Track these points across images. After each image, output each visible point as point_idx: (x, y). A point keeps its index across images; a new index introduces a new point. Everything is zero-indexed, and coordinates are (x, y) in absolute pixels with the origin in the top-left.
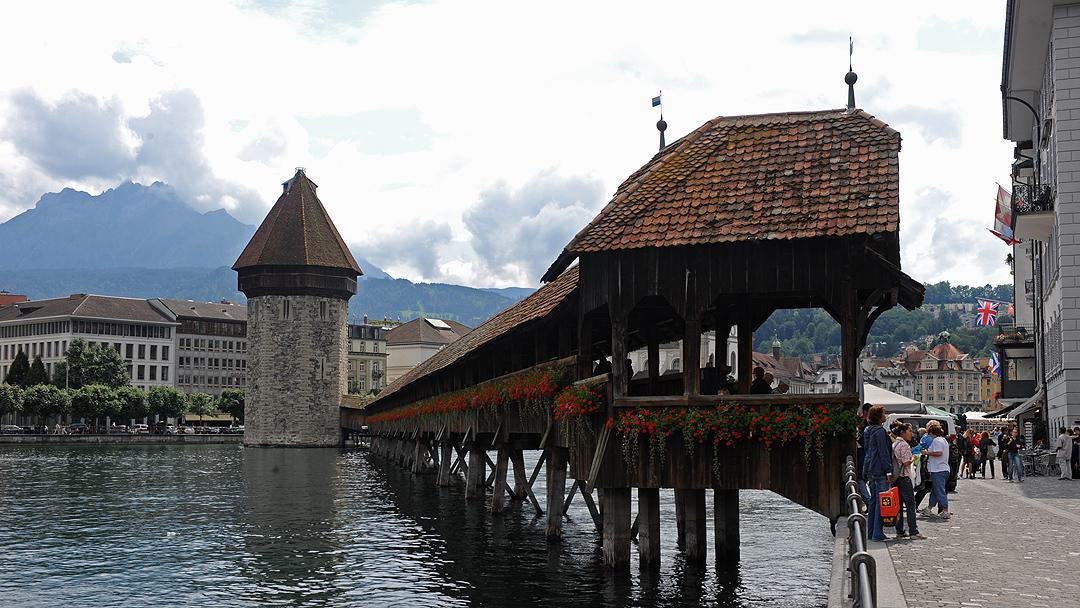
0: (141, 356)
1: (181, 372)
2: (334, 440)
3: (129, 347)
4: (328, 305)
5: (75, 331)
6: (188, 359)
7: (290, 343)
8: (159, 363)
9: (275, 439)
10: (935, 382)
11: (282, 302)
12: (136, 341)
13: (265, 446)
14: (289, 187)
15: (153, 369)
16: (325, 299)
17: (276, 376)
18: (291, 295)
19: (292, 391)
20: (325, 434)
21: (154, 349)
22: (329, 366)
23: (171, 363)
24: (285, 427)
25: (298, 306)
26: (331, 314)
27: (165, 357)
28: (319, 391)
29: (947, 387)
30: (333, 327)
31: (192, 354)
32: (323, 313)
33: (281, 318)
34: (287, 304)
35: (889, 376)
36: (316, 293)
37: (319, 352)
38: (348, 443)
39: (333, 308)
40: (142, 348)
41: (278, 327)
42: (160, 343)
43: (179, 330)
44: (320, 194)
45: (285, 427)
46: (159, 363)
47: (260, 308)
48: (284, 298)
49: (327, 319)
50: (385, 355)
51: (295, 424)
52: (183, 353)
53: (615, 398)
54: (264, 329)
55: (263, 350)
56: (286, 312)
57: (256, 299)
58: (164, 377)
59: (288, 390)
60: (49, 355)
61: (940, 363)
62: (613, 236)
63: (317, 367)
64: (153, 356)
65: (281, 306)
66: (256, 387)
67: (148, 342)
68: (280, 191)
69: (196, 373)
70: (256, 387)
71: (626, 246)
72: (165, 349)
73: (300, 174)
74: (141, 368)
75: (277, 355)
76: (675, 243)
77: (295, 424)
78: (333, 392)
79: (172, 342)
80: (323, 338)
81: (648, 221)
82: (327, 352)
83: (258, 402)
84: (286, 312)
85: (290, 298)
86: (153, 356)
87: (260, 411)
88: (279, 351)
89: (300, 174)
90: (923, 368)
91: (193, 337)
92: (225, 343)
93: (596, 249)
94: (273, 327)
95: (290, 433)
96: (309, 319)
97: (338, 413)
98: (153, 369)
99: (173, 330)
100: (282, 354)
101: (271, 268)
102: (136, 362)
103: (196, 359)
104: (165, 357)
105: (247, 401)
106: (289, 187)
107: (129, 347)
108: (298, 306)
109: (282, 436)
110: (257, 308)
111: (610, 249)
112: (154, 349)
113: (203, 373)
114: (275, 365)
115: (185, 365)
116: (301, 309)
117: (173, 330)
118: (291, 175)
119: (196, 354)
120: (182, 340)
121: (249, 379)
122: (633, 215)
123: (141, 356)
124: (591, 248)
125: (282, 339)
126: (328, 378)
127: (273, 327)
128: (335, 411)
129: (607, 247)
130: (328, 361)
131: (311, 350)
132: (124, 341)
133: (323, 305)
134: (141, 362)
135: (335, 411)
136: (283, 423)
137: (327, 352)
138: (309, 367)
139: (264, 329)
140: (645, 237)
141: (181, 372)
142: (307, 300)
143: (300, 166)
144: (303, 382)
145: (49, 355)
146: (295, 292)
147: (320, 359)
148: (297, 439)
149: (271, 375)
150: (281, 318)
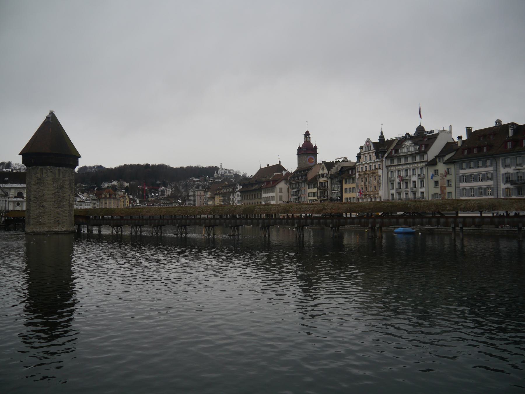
9: (55, 229)
17: (55, 201)
29: (112, 203)
33: (57, 176)
34: (59, 170)
45: (59, 224)
47: (44, 171)
51: (63, 222)
57: (40, 167)
61: (110, 195)
65: (57, 171)
66: (43, 206)
70: (43, 206)
73: (52, 113)
83: (44, 213)
85: (61, 168)
88: (56, 191)
89: (52, 113)
90: (103, 196)
100: (58, 192)
109: (57, 228)
136: (58, 222)
143: (52, 110)
146: (62, 166)
148: (64, 229)
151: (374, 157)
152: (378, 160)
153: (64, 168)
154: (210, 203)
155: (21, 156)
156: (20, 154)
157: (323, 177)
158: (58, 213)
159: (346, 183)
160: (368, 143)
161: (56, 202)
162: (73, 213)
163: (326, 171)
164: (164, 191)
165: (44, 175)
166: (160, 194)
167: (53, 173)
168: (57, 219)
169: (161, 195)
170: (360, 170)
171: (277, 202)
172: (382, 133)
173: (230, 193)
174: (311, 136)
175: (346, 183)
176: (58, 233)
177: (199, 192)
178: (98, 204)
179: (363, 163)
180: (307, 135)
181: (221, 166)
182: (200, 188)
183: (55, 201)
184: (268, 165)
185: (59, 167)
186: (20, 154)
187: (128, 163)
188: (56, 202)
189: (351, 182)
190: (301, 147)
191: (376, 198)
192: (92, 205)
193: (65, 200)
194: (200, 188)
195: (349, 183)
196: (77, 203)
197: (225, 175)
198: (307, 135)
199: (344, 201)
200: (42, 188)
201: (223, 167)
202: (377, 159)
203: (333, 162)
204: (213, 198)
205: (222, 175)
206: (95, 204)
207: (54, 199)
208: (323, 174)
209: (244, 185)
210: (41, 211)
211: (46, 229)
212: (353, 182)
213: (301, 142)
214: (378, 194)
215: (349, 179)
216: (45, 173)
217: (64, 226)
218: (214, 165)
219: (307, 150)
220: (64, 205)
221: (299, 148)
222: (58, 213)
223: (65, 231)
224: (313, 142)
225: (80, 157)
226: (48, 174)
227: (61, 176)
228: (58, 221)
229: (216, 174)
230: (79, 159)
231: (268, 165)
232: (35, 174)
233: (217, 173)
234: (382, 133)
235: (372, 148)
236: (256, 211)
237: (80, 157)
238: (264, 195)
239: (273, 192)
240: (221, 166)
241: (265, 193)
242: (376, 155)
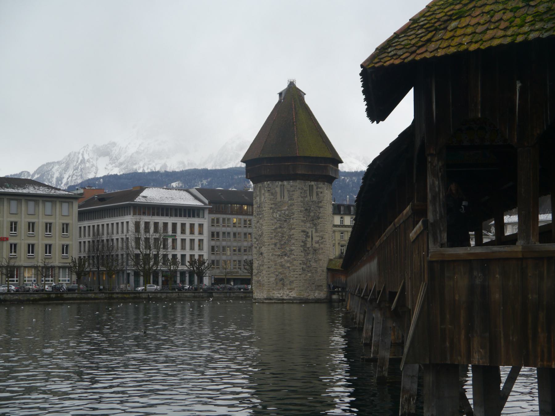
0: (183, 232)
1: (213, 243)
2: (321, 294)
3: (174, 225)
4: (315, 187)
5: (134, 214)
6: (218, 233)
7: (286, 218)
8: (196, 237)
9: (277, 294)
11: (279, 186)
12: (179, 221)
14: (283, 95)
15: (192, 241)
16: (313, 183)
17: (275, 244)
18: (286, 180)
19: (288, 257)
20: (316, 290)
21: (192, 226)
22: (317, 236)
23: (205, 236)
24: (283, 285)
25: (292, 189)
26: (317, 194)
27: (201, 233)
28: (310, 257)
30: (318, 204)
31: (221, 229)
32: (311, 194)
33: (279, 199)
36: (305, 178)
37: (308, 225)
38: (335, 297)
39: (319, 190)
40: (183, 225)
41: (276, 206)
42: (196, 221)
43: (211, 212)
44: (308, 100)
45: (283, 285)
46: (196, 237)
47: (263, 192)
48: (280, 183)
49: (315, 198)
51: (291, 282)
52: (216, 229)
53: (431, 250)
54: (266, 208)
55: (265, 223)
56: (282, 195)
57: (260, 185)
58: (201, 248)
59: (285, 255)
60: (117, 233)
62: (420, 44)
63: (307, 236)
64: (192, 232)
65: (278, 190)
67: (188, 221)
68: (276, 99)
69: (224, 243)
70: (261, 254)
71: (432, 55)
72: (201, 226)
73: (292, 85)
74: (183, 240)
75: (276, 228)
76: (496, 42)
77: (291, 282)
78: (321, 257)
79: (205, 221)
80: (312, 214)
81: (464, 21)
82: (315, 225)
84: (282, 195)
85: (285, 183)
86: (192, 232)
87: (264, 272)
89: (292, 85)
91: (221, 216)
92: (245, 221)
93: (397, 62)
94: (273, 206)
95: (288, 289)
96: (300, 199)
97: (325, 273)
98: (192, 241)
99: (206, 212)
100: (280, 227)
101: (270, 160)
102: (179, 236)
103: (224, 233)
104: (201, 233)
105: (255, 265)
106: (283, 95)
107: (174, 225)
108: (292, 189)
109: (281, 291)
110: (260, 191)
111: (413, 60)
112: (192, 226)
113: (229, 244)
114: (275, 236)
115: (215, 238)
116: (294, 191)
117: (206, 212)
118: (284, 86)
119: (224, 229)
120: (213, 220)
121: (256, 248)
122: (446, 18)
123: (183, 232)
124: (391, 62)
125: (280, 216)
126: (317, 246)
127: (273, 206)
128: (323, 271)
129: (410, 59)
130: (316, 231)
131: (303, 224)
132: (170, 220)
133: (311, 187)
134: (183, 237)
135: (323, 271)
136: (281, 282)
137: (315, 225)
138: (301, 236)
139: (266, 208)
140: (457, 40)
141: (213, 243)
142: (298, 184)
143: (292, 78)
144: (297, 249)
145: (117, 233)
147: (310, 231)
148: (293, 294)
149: (272, 244)
150: (279, 199)
158: (282, 266)
161: (278, 246)
167: (272, 194)
168: (281, 277)
183: (275, 244)
185: (282, 180)
188: (278, 246)
193: (293, 241)
200: (261, 221)
207: (274, 241)
217: (291, 289)
220: (292, 250)
222: (282, 266)
223: (295, 299)
227: (286, 198)
228: (282, 280)
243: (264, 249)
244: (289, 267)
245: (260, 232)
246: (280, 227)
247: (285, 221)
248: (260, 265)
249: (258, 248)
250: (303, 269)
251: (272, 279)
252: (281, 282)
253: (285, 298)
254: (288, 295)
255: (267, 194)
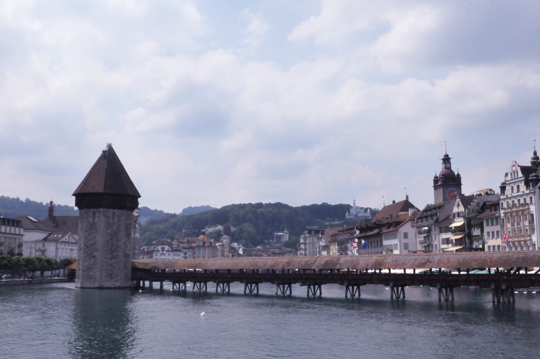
2: (130, 283)
9: (106, 284)
10: (201, 251)
13: (101, 288)
24: (111, 278)
33: (111, 220)
34: (114, 214)
35: (184, 248)
47: (97, 215)
50: (22, 235)
57: (92, 210)
59: (113, 258)
65: (111, 215)
70: (94, 257)
75: (108, 240)
83: (95, 265)
85: (116, 210)
94: (107, 225)
136: (110, 276)
143: (110, 142)
148: (118, 284)
150: (111, 220)
151: (523, 188)
152: (528, 192)
153: (120, 211)
154: (324, 253)
155: (74, 197)
156: (74, 195)
157: (459, 216)
158: (111, 265)
159: (488, 225)
160: (514, 168)
162: (130, 266)
163: (462, 209)
164: (280, 236)
165: (97, 219)
166: (275, 241)
168: (110, 272)
169: (276, 243)
170: (505, 206)
171: (401, 251)
172: (535, 153)
173: (347, 241)
174: (451, 161)
175: (488, 225)
176: (110, 288)
177: (311, 238)
178: (190, 253)
179: (509, 196)
180: (446, 160)
181: (354, 204)
182: (313, 232)
183: (107, 251)
184: (394, 202)
185: (114, 208)
186: (74, 195)
187: (237, 203)
189: (495, 223)
190: (438, 175)
191: (528, 247)
192: (182, 254)
193: (119, 249)
194: (313, 232)
195: (492, 224)
196: (164, 252)
197: (359, 215)
198: (446, 160)
199: (486, 249)
200: (94, 235)
201: (356, 205)
202: (527, 189)
203: (473, 196)
204: (326, 248)
205: (356, 216)
206: (185, 253)
208: (458, 213)
209: (362, 230)
210: (91, 263)
211: (97, 285)
212: (497, 224)
213: (439, 169)
214: (531, 240)
215: (492, 220)
216: (98, 217)
218: (345, 202)
219: (448, 181)
221: (436, 177)
222: (111, 265)
224: (455, 169)
225: (140, 196)
226: (101, 217)
227: (116, 221)
228: (110, 275)
229: (347, 214)
230: (139, 199)
231: (394, 202)
232: (87, 218)
233: (349, 213)
234: (535, 153)
235: (520, 175)
236: (340, 264)
237: (140, 196)
238: (386, 243)
239: (396, 238)
240: (354, 204)
241: (386, 239)
242: (525, 184)
243: (96, 254)
244: (115, 266)
245: (92, 242)
246: (111, 239)
247: (115, 236)
248: (92, 265)
249: (89, 252)
250: (124, 268)
251: (104, 274)
252: (110, 276)
253: (112, 287)
254: (114, 285)
255: (102, 217)
